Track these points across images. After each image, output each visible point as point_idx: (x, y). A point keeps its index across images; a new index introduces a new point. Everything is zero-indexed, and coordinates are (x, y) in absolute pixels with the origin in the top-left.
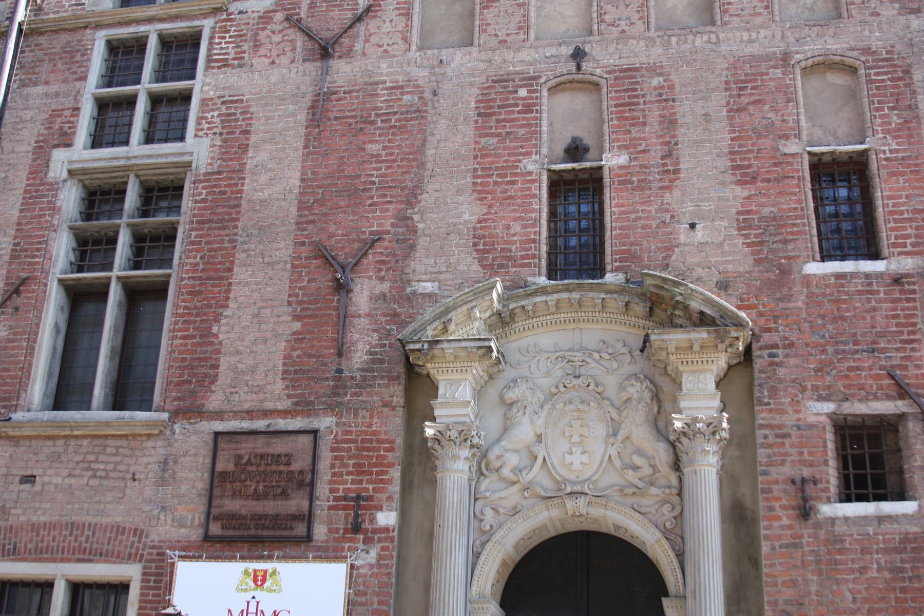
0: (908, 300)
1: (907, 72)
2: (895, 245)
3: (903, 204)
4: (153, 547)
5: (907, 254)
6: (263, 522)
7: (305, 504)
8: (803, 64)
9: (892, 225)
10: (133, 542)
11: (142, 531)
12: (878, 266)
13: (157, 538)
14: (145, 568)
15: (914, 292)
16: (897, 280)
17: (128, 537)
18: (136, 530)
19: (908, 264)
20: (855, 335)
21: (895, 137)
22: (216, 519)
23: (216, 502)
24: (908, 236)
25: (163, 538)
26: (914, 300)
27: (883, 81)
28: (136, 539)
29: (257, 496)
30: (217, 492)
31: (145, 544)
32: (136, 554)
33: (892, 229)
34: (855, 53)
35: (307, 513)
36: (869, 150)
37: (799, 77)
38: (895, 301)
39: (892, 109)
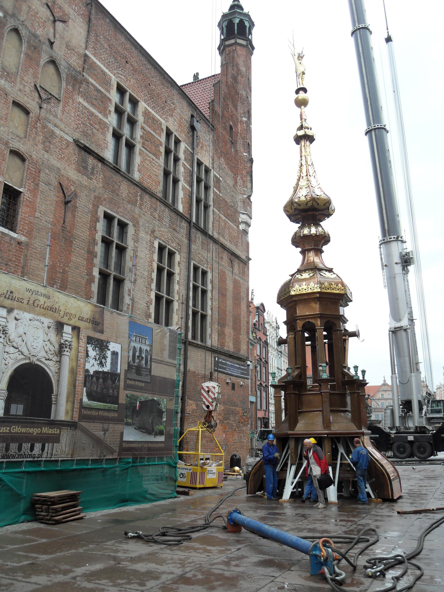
0: (21, 251)
1: (39, 172)
2: (21, 230)
3: (27, 217)
5: (24, 235)
8: (11, 148)
9: (22, 223)
12: (12, 234)
15: (22, 249)
16: (19, 243)
19: (23, 239)
20: (2, 257)
21: (30, 193)
24: (25, 229)
26: (22, 252)
27: (32, 170)
33: (22, 225)
34: (27, 156)
36: (22, 192)
37: (8, 152)
38: (17, 250)
39: (32, 182)
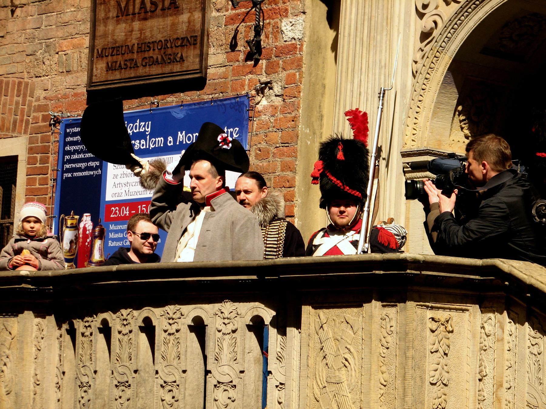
4: (40, 108)
6: (151, 53)
7: (197, 15)
10: (17, 103)
11: (27, 84)
13: (43, 94)
14: (31, 141)
17: (12, 96)
18: (20, 83)
22: (101, 56)
23: (101, 29)
25: (49, 94)
28: (20, 99)
29: (145, 14)
30: (101, 15)
31: (30, 106)
32: (22, 121)
35: (200, 33)
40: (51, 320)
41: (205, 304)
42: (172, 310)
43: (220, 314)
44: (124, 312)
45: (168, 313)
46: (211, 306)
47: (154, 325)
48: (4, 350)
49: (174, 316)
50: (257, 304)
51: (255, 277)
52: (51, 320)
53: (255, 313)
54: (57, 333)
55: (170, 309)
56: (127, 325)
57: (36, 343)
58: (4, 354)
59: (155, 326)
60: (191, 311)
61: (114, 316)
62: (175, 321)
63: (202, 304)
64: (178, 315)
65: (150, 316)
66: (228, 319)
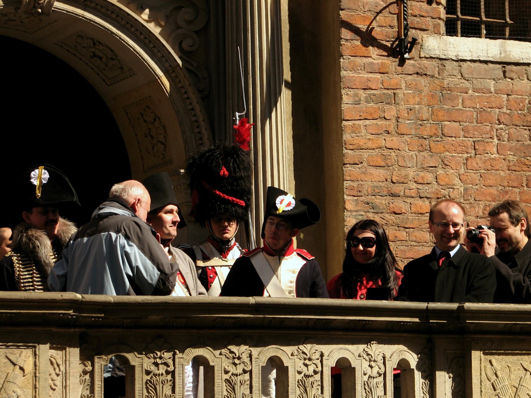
40: (74, 353)
41: (349, 344)
42: (309, 349)
43: (365, 356)
44: (233, 348)
45: (304, 353)
46: (355, 346)
47: (285, 365)
48: (15, 390)
49: (313, 357)
50: (402, 347)
51: (417, 320)
52: (74, 353)
53: (401, 358)
54: (81, 368)
55: (307, 348)
56: (240, 364)
57: (50, 382)
58: (15, 394)
59: (287, 367)
60: (334, 353)
61: (217, 352)
62: (314, 362)
63: (345, 344)
64: (317, 355)
65: (279, 355)
66: (375, 361)
